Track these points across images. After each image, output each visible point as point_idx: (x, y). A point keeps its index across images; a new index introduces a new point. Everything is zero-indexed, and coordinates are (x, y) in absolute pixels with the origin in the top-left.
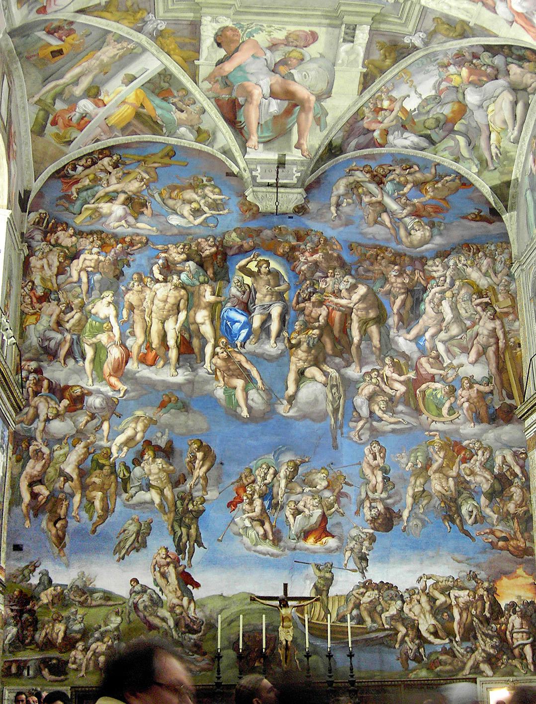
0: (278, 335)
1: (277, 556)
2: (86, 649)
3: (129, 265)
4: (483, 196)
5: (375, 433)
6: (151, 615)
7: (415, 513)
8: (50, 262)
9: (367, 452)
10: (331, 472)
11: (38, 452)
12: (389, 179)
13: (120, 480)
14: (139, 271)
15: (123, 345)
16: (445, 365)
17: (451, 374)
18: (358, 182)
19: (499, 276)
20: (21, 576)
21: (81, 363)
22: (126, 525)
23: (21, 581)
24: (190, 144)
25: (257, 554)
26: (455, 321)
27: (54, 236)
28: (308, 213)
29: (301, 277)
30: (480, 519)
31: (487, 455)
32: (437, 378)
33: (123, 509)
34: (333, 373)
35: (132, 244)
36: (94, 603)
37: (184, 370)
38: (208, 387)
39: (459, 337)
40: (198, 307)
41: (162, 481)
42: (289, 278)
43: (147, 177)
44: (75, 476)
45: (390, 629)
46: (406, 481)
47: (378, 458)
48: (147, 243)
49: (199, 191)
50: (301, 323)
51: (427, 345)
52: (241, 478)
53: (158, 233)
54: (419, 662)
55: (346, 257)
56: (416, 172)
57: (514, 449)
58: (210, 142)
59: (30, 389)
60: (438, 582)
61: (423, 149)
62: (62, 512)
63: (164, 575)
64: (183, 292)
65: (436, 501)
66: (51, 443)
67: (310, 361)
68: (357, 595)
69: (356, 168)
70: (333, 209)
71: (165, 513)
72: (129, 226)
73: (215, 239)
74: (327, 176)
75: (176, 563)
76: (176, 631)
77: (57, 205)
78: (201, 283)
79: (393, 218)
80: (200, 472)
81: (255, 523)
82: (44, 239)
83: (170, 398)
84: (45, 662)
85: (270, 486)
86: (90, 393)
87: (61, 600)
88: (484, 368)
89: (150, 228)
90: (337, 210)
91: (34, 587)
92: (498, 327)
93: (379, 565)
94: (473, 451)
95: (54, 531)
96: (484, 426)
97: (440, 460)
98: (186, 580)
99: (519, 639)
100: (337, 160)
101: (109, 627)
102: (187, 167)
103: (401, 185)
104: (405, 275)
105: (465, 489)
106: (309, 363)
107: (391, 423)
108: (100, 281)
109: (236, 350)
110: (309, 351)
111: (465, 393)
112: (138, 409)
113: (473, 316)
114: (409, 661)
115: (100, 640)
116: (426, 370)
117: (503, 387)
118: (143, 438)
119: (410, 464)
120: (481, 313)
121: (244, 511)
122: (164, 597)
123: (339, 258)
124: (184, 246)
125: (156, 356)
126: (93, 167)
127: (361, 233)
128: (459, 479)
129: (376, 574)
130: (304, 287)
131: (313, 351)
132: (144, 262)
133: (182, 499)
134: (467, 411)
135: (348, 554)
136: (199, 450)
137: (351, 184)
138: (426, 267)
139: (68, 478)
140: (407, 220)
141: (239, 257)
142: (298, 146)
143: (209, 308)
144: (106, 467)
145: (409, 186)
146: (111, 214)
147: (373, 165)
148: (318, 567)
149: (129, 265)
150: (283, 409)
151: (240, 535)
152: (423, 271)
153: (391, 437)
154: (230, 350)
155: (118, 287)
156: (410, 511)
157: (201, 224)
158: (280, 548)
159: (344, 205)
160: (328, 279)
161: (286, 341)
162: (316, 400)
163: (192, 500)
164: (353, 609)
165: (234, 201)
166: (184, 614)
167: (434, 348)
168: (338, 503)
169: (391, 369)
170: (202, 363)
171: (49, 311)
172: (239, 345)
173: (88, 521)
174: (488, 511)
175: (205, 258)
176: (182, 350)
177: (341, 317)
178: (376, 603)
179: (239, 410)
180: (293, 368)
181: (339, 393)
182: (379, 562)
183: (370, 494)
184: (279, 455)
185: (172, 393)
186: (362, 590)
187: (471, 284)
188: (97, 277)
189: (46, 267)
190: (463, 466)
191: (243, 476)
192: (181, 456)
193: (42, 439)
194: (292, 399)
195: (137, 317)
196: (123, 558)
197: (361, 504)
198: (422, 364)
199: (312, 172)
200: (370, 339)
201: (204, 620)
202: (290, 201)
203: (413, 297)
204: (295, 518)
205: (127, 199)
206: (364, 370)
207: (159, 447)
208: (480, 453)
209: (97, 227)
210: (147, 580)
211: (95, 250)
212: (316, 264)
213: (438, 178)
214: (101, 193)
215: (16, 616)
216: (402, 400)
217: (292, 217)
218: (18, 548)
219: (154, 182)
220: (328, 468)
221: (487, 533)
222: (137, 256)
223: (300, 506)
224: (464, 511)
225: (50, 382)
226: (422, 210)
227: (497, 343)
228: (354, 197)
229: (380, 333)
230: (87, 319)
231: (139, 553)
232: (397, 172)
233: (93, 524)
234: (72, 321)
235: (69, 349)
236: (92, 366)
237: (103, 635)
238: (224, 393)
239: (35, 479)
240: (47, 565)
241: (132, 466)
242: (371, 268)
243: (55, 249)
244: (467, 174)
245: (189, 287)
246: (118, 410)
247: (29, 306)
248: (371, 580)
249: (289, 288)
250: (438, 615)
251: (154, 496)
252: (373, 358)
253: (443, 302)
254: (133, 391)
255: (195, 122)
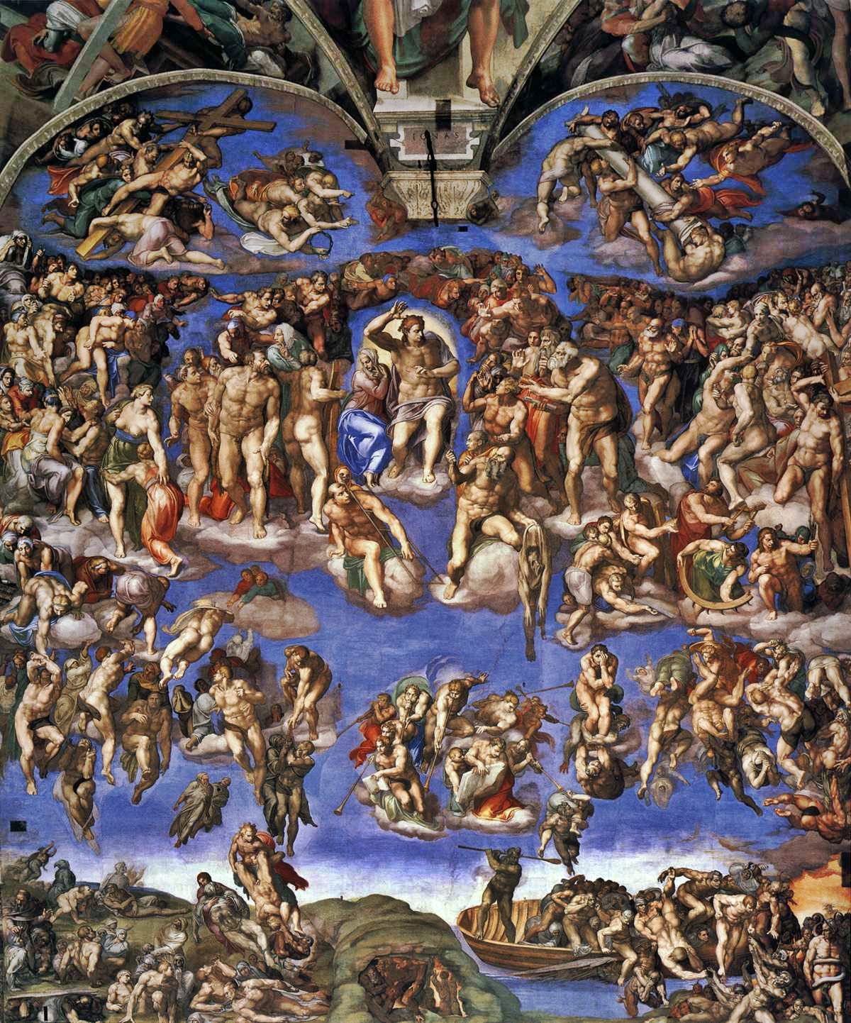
0: (437, 459)
1: (431, 837)
2: (132, 982)
3: (177, 336)
4: (830, 164)
5: (600, 631)
6: (231, 929)
7: (663, 768)
8: (41, 332)
9: (584, 662)
10: (523, 699)
11: (41, 670)
12: (650, 139)
13: (175, 716)
14: (196, 345)
15: (172, 482)
16: (731, 507)
17: (741, 522)
18: (591, 149)
19: (844, 330)
20: (26, 871)
21: (103, 518)
22: (188, 790)
23: (27, 878)
24: (276, 85)
25: (398, 835)
26: (756, 424)
27: (44, 283)
28: (495, 218)
29: (480, 348)
30: (775, 777)
31: (795, 667)
32: (715, 531)
33: (184, 764)
34: (531, 525)
35: (180, 292)
36: (142, 912)
37: (277, 527)
38: (320, 556)
39: (762, 454)
40: (299, 410)
41: (244, 718)
42: (459, 351)
43: (202, 157)
44: (103, 710)
45: (611, 955)
46: (648, 715)
47: (604, 674)
48: (206, 291)
49: (298, 182)
50: (478, 435)
51: (702, 470)
52: (372, 712)
53: (225, 271)
54: (655, 1007)
55: (566, 306)
56: (703, 121)
57: (841, 657)
58: (311, 80)
59: (21, 565)
60: (693, 880)
61: (719, 71)
62: (86, 769)
63: (251, 869)
64: (272, 383)
65: (699, 749)
66: (61, 656)
67: (492, 505)
68: (559, 901)
69: (587, 119)
70: (542, 208)
71: (251, 770)
72: (175, 258)
73: (326, 277)
74: (532, 140)
75: (268, 849)
76: (271, 954)
77: (44, 222)
78: (306, 365)
79: (654, 220)
80: (305, 701)
81: (394, 785)
82: (26, 288)
83: (254, 577)
84: (70, 1001)
85: (420, 724)
86: (121, 570)
87: (92, 907)
88: (801, 510)
89: (208, 259)
90: (550, 209)
91: (47, 888)
92: (834, 432)
93: (596, 852)
94: (770, 660)
95: (74, 799)
96: (793, 617)
97: (711, 678)
98: (285, 879)
99: (823, 974)
100: (553, 105)
101: (166, 948)
102: (276, 133)
103: (672, 152)
104: (669, 337)
105: (751, 727)
106: (490, 510)
107: (629, 614)
108: (128, 367)
109: (364, 488)
110: (490, 487)
111: (764, 558)
112: (201, 597)
113: (791, 412)
114: (639, 1005)
115: (154, 967)
116: (696, 518)
117: (833, 544)
118: (211, 645)
119: (658, 685)
120: (806, 406)
121: (377, 766)
122: (250, 903)
123: (550, 304)
124: (273, 293)
125: (230, 500)
126: (103, 142)
127: (592, 256)
128: (741, 711)
129: (592, 867)
130: (484, 366)
131: (497, 488)
132: (202, 327)
133: (277, 746)
134: (766, 589)
135: (546, 835)
136: (303, 665)
137: (577, 153)
138: (710, 319)
139: (92, 714)
140: (680, 224)
141: (370, 312)
142: (474, 82)
143: (317, 413)
144: (154, 696)
145: (689, 152)
146: (140, 235)
147: (622, 110)
148: (495, 855)
149: (177, 336)
150: (444, 591)
151: (370, 804)
152: (704, 326)
153: (629, 639)
154: (354, 488)
155: (159, 377)
156: (654, 765)
157: (300, 249)
158: (435, 826)
159: (563, 198)
160: (528, 350)
161: (451, 470)
162: (500, 576)
163: (293, 747)
164: (551, 923)
165: (363, 197)
166: (283, 927)
167: (715, 475)
168: (534, 751)
169: (635, 517)
170: (307, 514)
171: (44, 424)
172: (369, 478)
173: (127, 783)
174: (789, 765)
175: (309, 315)
176: (272, 490)
177: (549, 421)
178: (590, 915)
179: (369, 595)
180: (462, 518)
181: (540, 562)
182: (597, 848)
183: (586, 735)
184: (435, 673)
185: (258, 569)
186: (567, 893)
187: (792, 350)
188: (123, 359)
189: (33, 342)
190: (750, 688)
191: (376, 707)
192: (275, 675)
193: (46, 649)
194: (459, 575)
195: (194, 433)
196: (185, 841)
197: (571, 753)
198: (689, 507)
199: (504, 133)
200: (599, 461)
201: (314, 937)
202: (460, 197)
203: (681, 378)
204: (460, 777)
205: (166, 204)
206: (586, 520)
207: (238, 660)
208: (783, 664)
209: (117, 262)
210: (223, 875)
211: (117, 307)
212: (507, 320)
213: (747, 130)
214: (121, 194)
215: (23, 930)
216: (651, 572)
217: (464, 229)
218: (18, 827)
219: (214, 167)
220: (518, 693)
221: (783, 802)
222: (190, 317)
223: (470, 756)
224: (747, 763)
225: (53, 553)
226: (710, 202)
227: (829, 462)
228: (583, 181)
229: (618, 450)
230: (110, 438)
231: (211, 835)
232: (667, 123)
233: (137, 788)
234: (85, 442)
235: (81, 494)
236: (121, 521)
237: (158, 960)
238: (344, 566)
239: (39, 716)
240: (66, 853)
241: (194, 692)
242: (608, 325)
243: (46, 308)
244: (805, 119)
245: (282, 374)
246: (168, 598)
247: (9, 417)
248: (582, 877)
249: (457, 370)
250: (690, 932)
251: (231, 741)
252: (603, 497)
253: (738, 388)
254: (192, 564)
255: (277, 37)
